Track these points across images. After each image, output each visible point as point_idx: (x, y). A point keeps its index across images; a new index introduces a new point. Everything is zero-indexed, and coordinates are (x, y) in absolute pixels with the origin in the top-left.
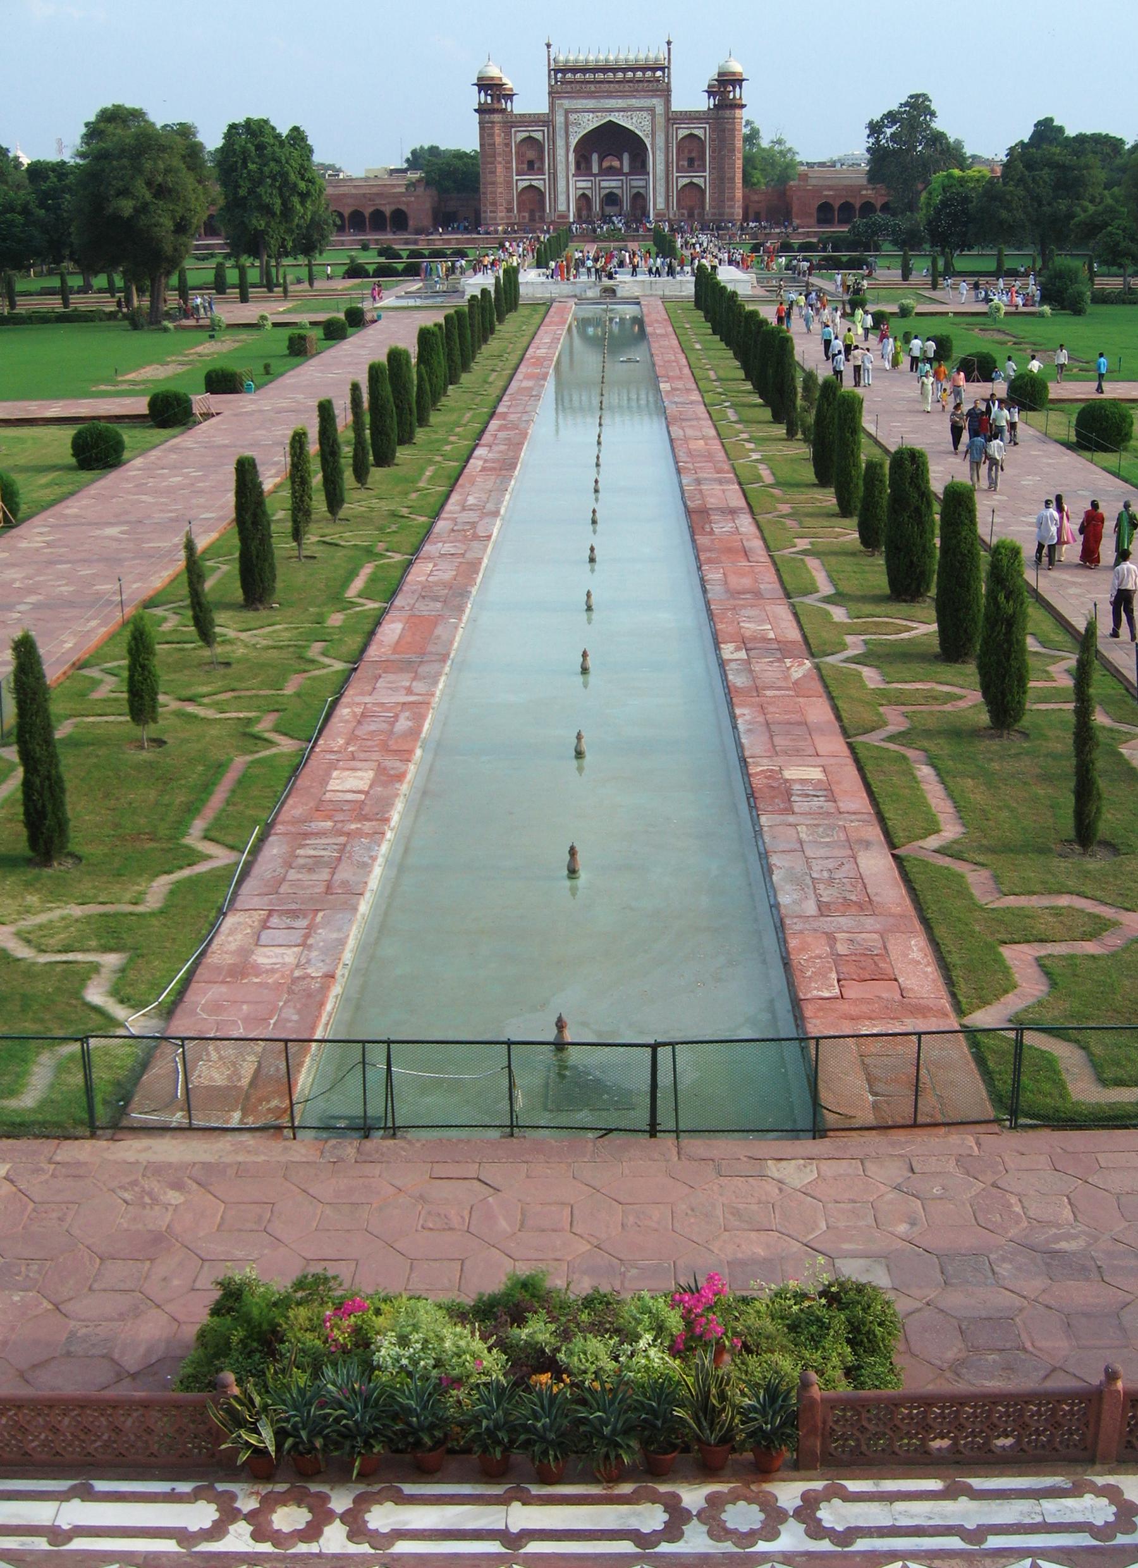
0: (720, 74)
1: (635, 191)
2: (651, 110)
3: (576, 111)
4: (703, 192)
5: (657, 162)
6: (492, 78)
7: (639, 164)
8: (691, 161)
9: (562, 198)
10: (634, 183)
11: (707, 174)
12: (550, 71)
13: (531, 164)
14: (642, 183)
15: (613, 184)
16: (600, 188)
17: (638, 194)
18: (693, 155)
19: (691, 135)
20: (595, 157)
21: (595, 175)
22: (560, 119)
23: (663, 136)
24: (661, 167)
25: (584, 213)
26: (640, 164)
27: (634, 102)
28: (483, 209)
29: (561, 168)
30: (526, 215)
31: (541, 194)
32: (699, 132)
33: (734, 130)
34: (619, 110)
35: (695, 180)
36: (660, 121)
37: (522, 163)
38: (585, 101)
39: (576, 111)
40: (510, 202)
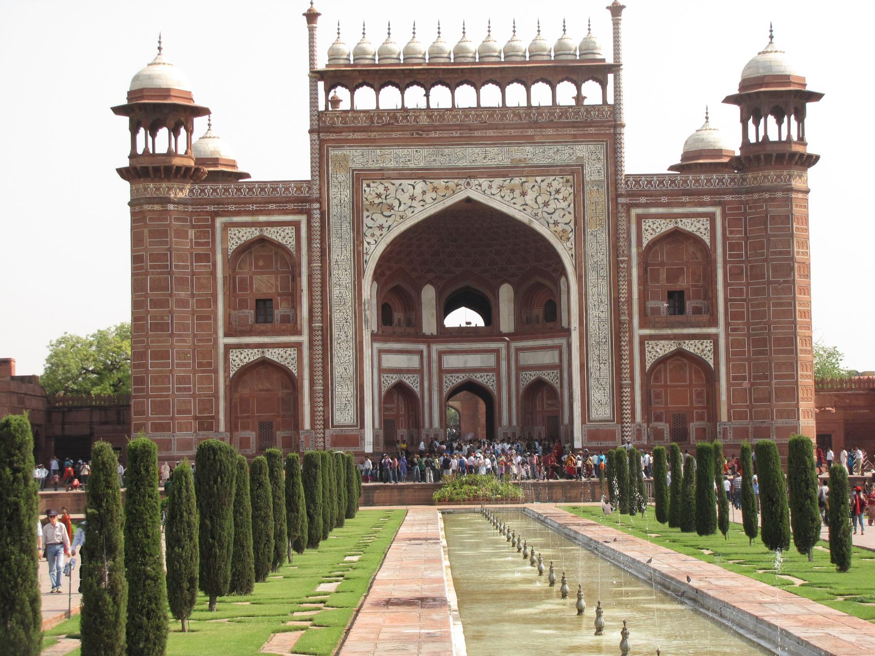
0: (745, 84)
1: (530, 377)
2: (574, 172)
3: (381, 175)
4: (710, 376)
5: (587, 300)
6: (166, 92)
7: (538, 312)
8: (676, 299)
9: (343, 393)
10: (529, 359)
11: (720, 330)
12: (316, 75)
13: (264, 306)
14: (549, 358)
15: (474, 361)
16: (441, 371)
17: (539, 385)
18: (683, 283)
19: (676, 236)
20: (429, 294)
21: (428, 340)
22: (340, 195)
23: (603, 237)
24: (599, 315)
25: (402, 432)
26: (543, 312)
27: (529, 153)
28: (135, 419)
29: (341, 316)
30: (252, 435)
31: (291, 382)
32: (697, 227)
33: (788, 219)
34: (493, 173)
35: (690, 347)
36: (597, 200)
37: (243, 304)
38: (402, 152)
39: (381, 175)
40: (209, 403)
